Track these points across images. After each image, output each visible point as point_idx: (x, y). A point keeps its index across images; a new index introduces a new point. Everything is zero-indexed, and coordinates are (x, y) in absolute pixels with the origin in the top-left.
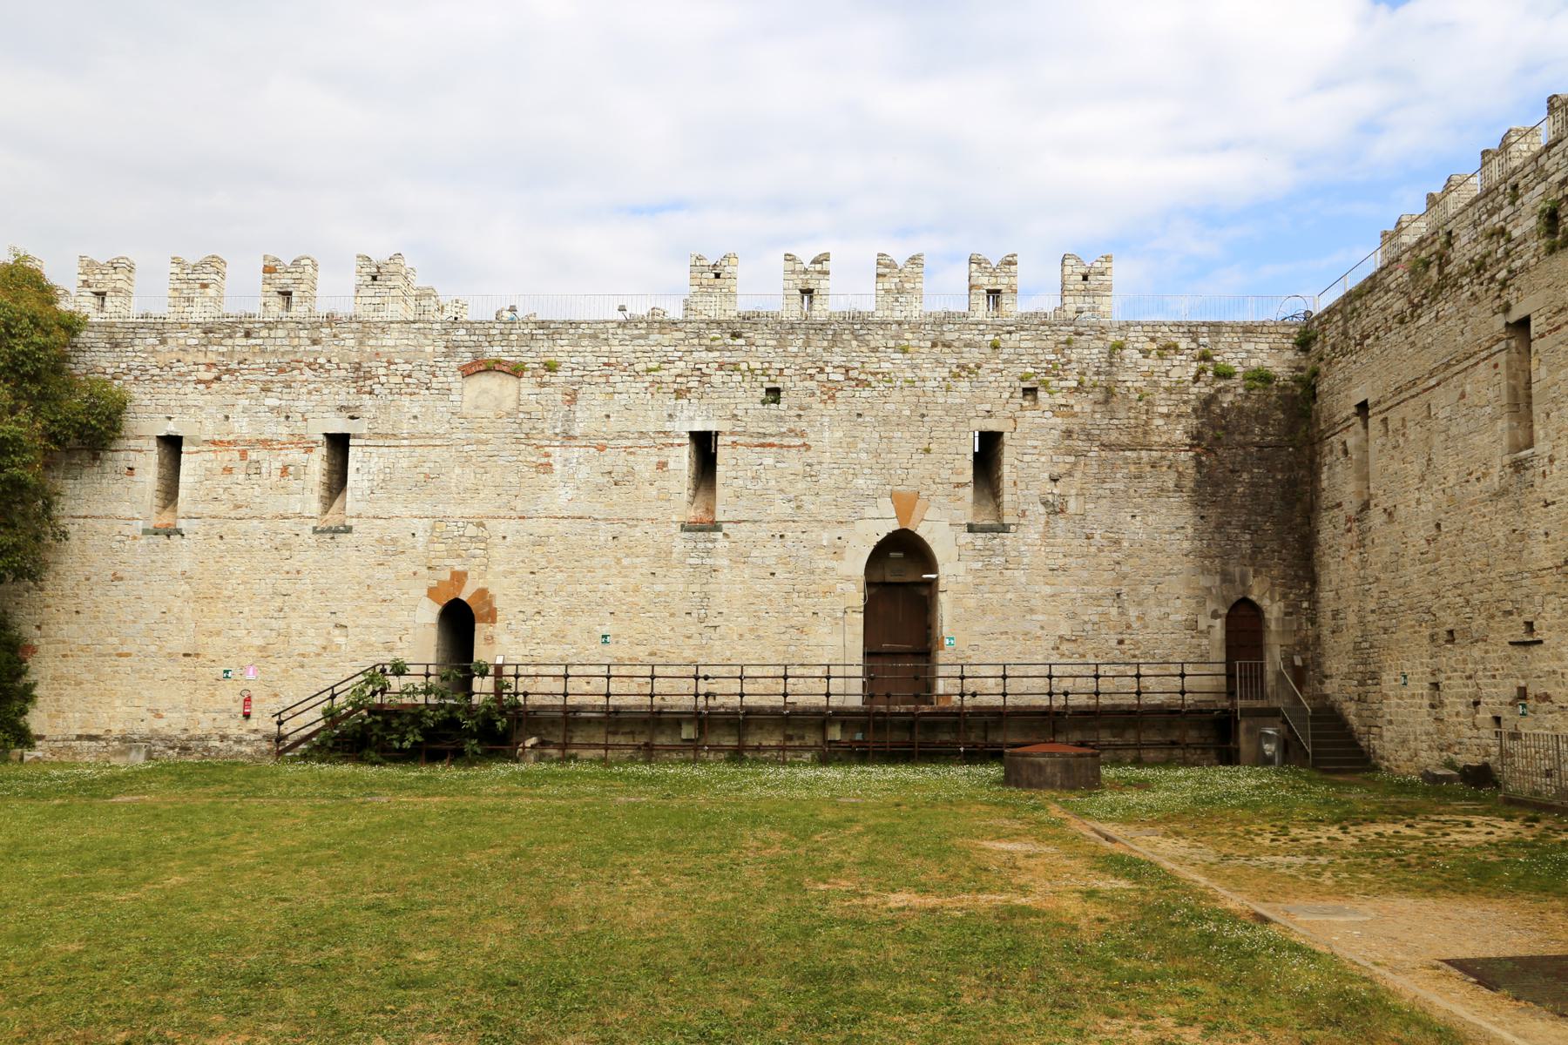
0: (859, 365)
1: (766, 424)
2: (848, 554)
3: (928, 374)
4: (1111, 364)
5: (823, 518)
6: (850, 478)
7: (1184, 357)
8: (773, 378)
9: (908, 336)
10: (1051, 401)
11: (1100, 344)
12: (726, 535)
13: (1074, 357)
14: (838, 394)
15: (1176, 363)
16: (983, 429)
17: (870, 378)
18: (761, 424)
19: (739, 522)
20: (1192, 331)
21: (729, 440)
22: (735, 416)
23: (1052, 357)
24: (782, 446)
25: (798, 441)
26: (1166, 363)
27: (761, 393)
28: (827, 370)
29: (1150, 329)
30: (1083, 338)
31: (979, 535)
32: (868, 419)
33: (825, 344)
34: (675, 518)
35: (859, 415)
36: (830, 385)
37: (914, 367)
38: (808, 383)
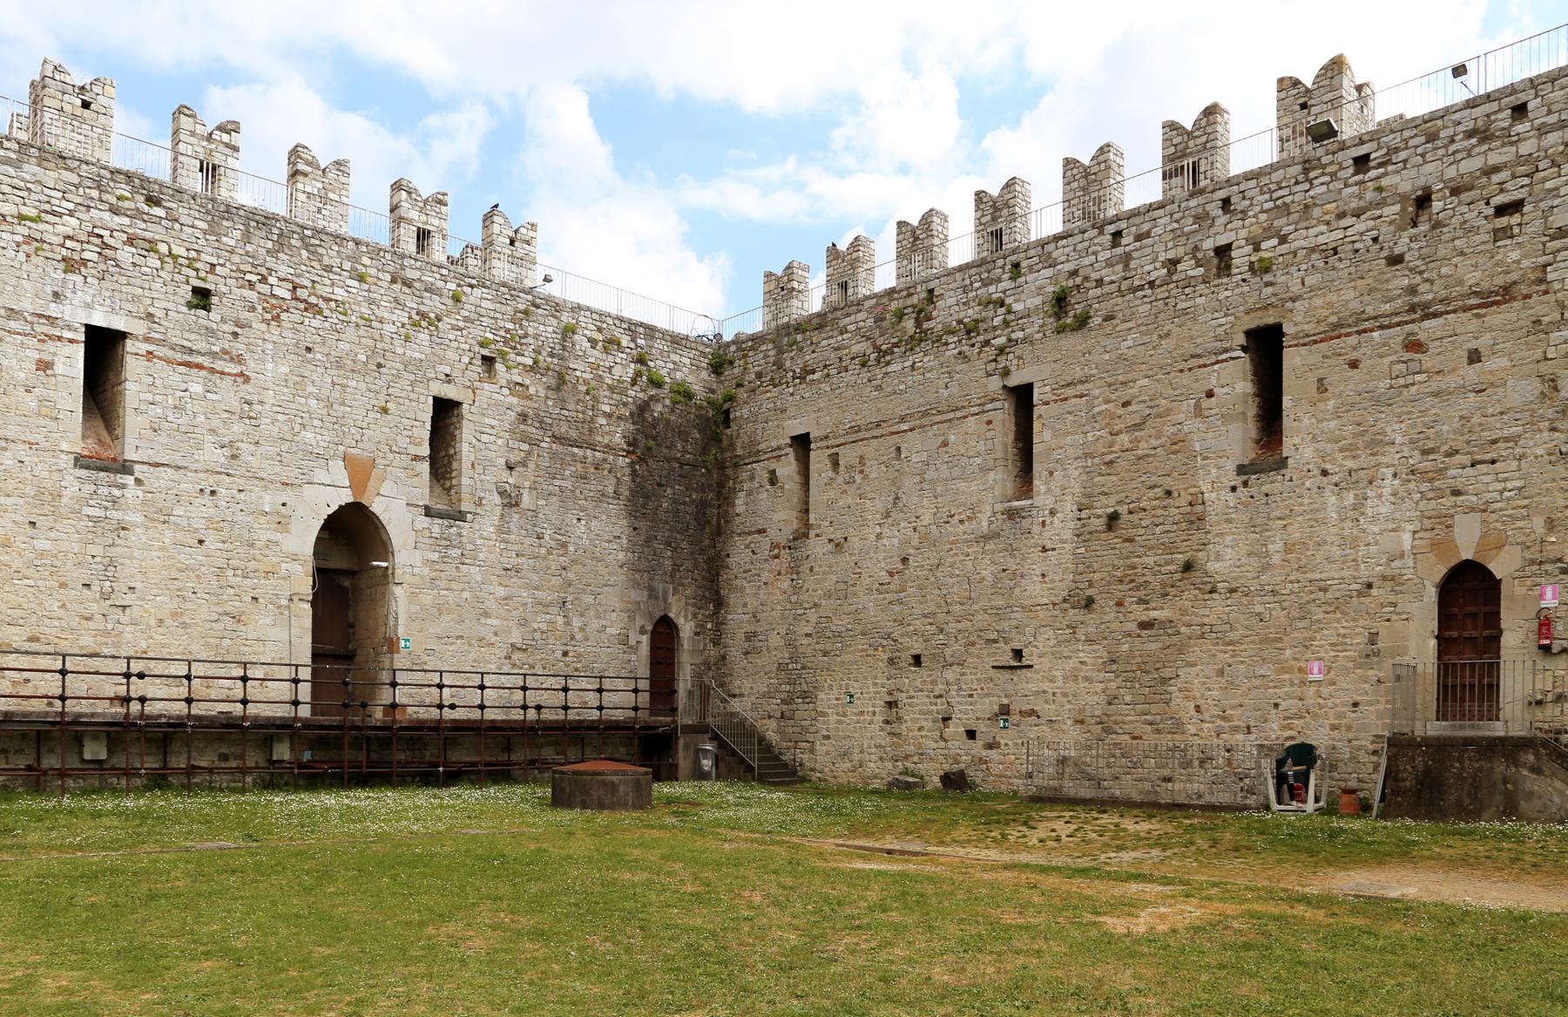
0: (309, 284)
1: (192, 337)
2: (295, 526)
3: (386, 315)
4: (564, 348)
5: (263, 475)
6: (297, 429)
7: (624, 356)
8: (202, 274)
9: (365, 260)
10: (508, 376)
11: (555, 322)
12: (138, 482)
13: (531, 331)
14: (284, 316)
15: (618, 360)
16: (442, 395)
17: (322, 304)
18: (187, 335)
19: (157, 465)
20: (632, 327)
21: (144, 347)
22: (150, 315)
23: (510, 326)
24: (212, 371)
25: (233, 368)
26: (610, 358)
27: (186, 292)
28: (272, 280)
29: (597, 317)
30: (540, 311)
31: (437, 521)
32: (318, 356)
33: (270, 245)
34: (64, 446)
35: (309, 349)
36: (273, 301)
37: (371, 302)
38: (246, 293)
